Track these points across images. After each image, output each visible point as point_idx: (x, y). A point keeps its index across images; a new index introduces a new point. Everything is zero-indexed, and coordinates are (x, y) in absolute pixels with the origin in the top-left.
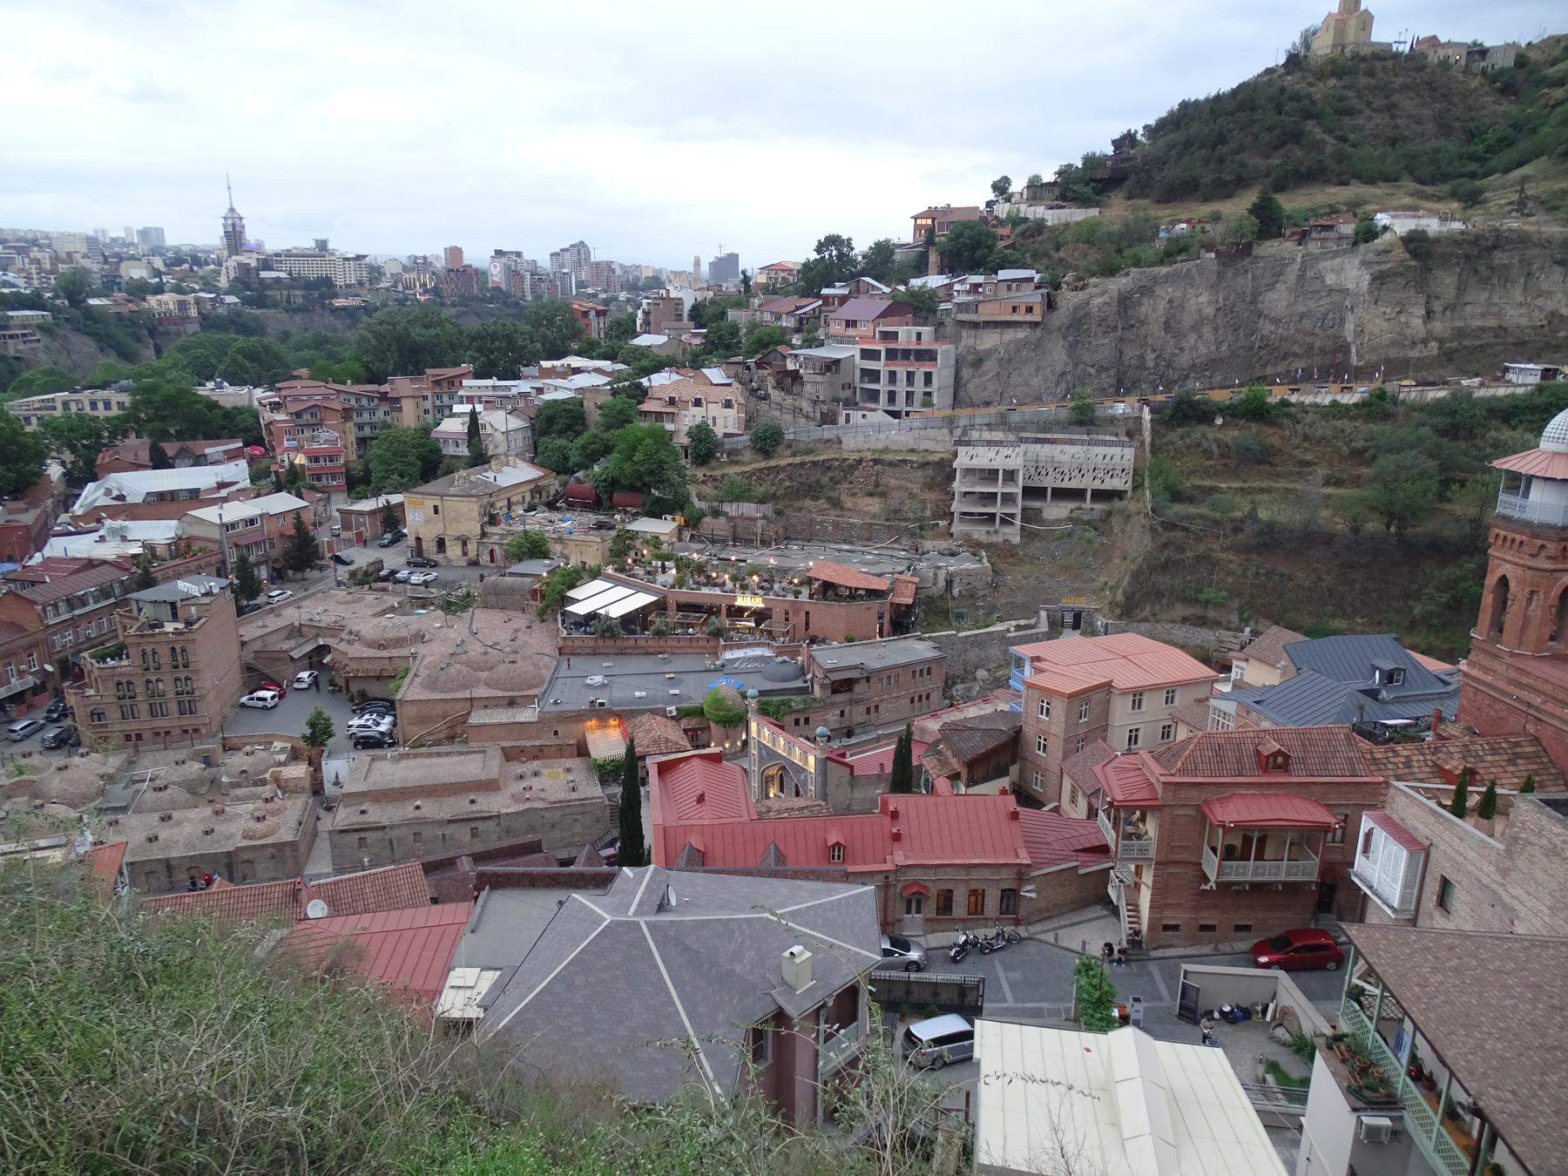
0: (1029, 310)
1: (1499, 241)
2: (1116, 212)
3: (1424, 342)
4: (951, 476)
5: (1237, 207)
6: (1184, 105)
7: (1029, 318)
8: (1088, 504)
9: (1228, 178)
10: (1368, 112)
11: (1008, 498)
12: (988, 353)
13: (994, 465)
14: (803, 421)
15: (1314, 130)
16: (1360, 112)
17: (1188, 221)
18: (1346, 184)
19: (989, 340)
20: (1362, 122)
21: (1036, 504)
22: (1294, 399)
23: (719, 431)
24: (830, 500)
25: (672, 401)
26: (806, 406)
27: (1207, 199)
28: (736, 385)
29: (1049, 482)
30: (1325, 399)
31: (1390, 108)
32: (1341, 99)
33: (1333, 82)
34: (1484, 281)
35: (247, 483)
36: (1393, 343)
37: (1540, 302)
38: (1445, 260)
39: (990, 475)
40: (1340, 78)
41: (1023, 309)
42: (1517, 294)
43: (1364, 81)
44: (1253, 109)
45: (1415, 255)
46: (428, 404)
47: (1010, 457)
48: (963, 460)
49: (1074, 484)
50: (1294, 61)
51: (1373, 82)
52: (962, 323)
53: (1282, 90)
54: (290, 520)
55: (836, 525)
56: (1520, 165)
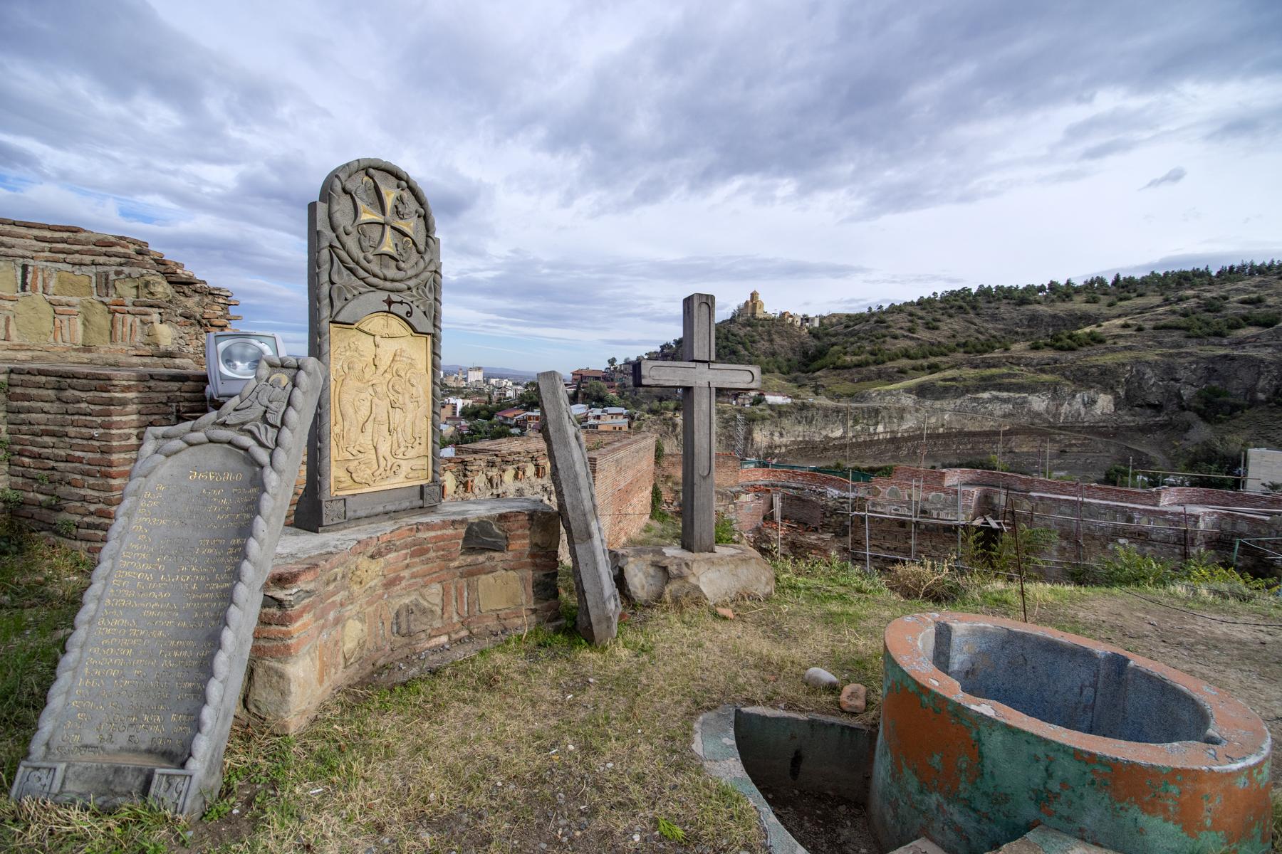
15: (740, 347)
31: (771, 341)
34: (799, 422)
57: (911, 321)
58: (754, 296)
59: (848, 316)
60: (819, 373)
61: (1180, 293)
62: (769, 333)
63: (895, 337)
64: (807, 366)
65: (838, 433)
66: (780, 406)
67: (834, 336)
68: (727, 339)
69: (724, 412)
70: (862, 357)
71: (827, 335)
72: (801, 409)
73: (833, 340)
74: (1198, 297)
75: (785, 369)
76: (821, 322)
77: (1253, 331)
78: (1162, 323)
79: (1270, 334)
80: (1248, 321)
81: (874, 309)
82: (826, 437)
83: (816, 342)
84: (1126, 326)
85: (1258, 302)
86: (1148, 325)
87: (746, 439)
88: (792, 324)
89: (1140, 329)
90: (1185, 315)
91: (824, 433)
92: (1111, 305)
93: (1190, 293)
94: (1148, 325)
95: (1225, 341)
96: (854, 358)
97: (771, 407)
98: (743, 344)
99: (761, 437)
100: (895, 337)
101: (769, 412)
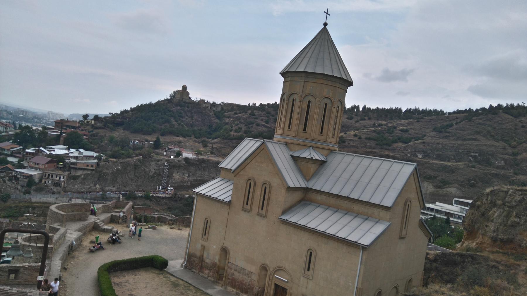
0: (92, 166)
1: (203, 161)
3: (188, 182)
5: (151, 139)
7: (91, 168)
9: (150, 130)
10: (186, 117)
12: (79, 176)
14: (18, 192)
15: (172, 119)
18: (178, 136)
19: (79, 173)
20: (184, 119)
26: (19, 187)
27: (144, 134)
31: (192, 117)
32: (181, 113)
33: (179, 107)
34: (200, 170)
36: (181, 181)
40: (181, 107)
41: (90, 166)
42: (207, 173)
43: (186, 109)
45: (186, 162)
53: (166, 108)
56: (216, 138)
57: (268, 117)
58: (184, 88)
59: (239, 106)
60: (216, 140)
61: (380, 122)
63: (258, 125)
64: (210, 134)
67: (229, 117)
70: (240, 134)
71: (224, 116)
73: (227, 120)
74: (386, 125)
76: (222, 109)
77: (400, 145)
78: (369, 136)
79: (404, 147)
80: (400, 140)
81: (251, 105)
83: (218, 121)
84: (355, 135)
85: (406, 131)
86: (363, 137)
88: (205, 108)
89: (360, 138)
90: (378, 133)
92: (357, 122)
93: (384, 122)
94: (363, 137)
95: (390, 148)
96: (235, 134)
97: (186, 159)
100: (258, 125)
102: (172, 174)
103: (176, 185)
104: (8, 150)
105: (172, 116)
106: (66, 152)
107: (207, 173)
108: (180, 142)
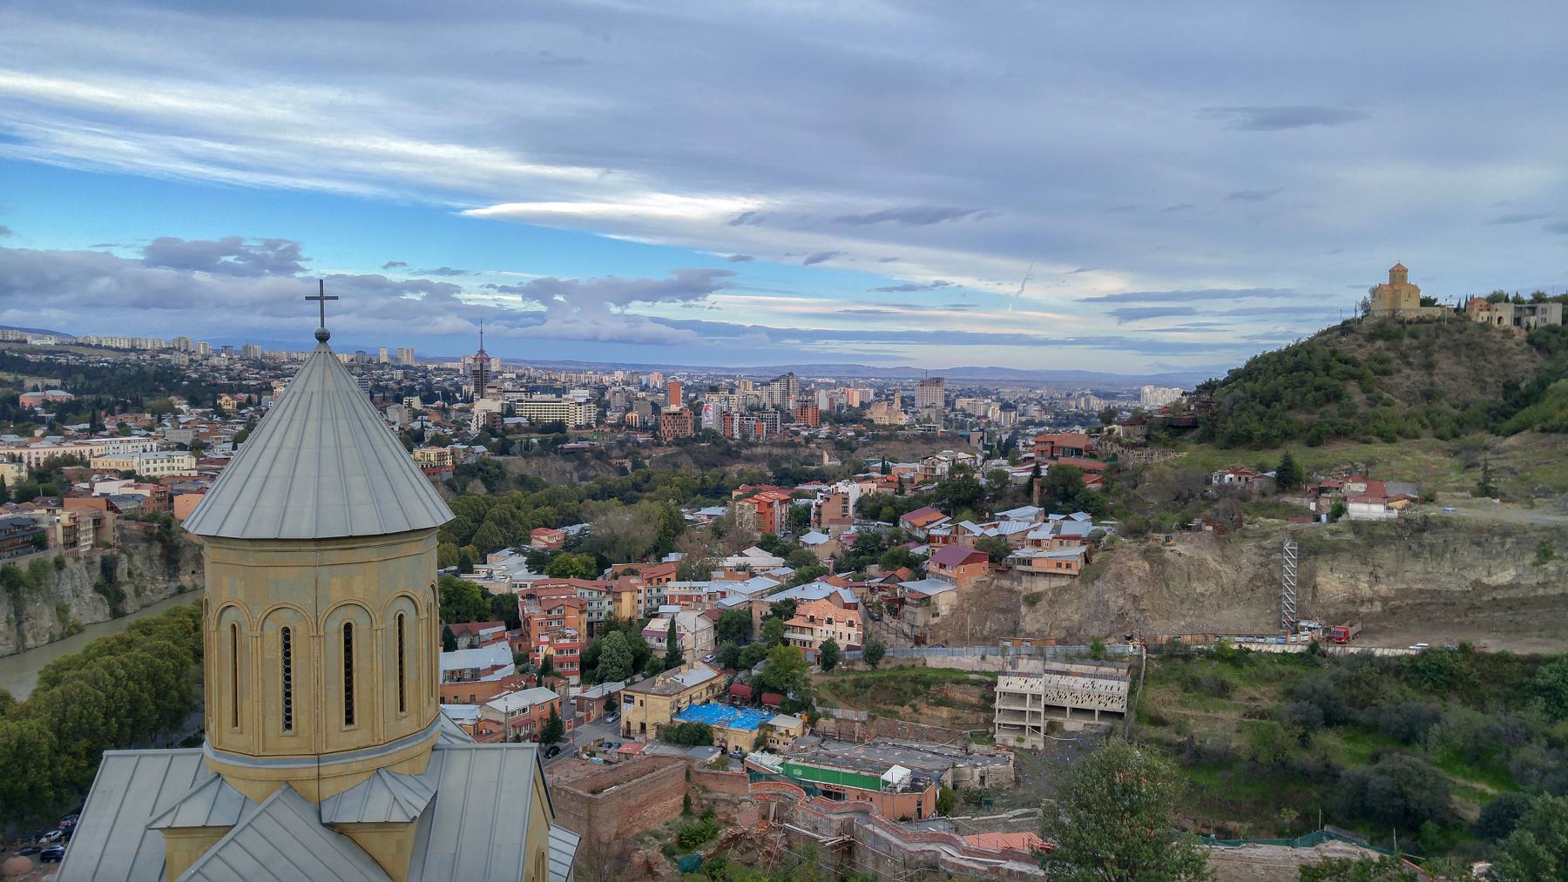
2: (1186, 456)
4: (993, 700)
5: (1274, 458)
6: (1255, 360)
7: (1068, 572)
8: (1096, 721)
10: (1408, 371)
11: (1035, 714)
13: (1024, 691)
15: (1352, 388)
16: (1399, 371)
17: (1235, 471)
19: (1041, 585)
21: (1059, 719)
22: (1253, 647)
23: (842, 644)
24: (913, 706)
25: (812, 619)
27: (1259, 448)
28: (861, 607)
29: (1068, 703)
30: (1278, 649)
33: (1380, 343)
34: (1416, 556)
35: (510, 669)
37: (1466, 573)
38: (1385, 540)
39: (1023, 696)
42: (1447, 568)
44: (1308, 369)
46: (641, 596)
47: (1037, 686)
48: (1003, 684)
49: (1085, 706)
50: (1346, 328)
51: (1415, 342)
52: (1023, 572)
53: (1334, 353)
54: (548, 708)
55: (911, 728)
56: (1515, 432)
62: (1427, 350)
65: (1505, 576)
66: (1373, 524)
68: (1327, 369)
69: (1266, 536)
72: (1421, 530)
75: (1445, 430)
82: (1477, 583)
87: (1301, 583)
91: (1472, 576)
97: (1357, 526)
98: (1359, 378)
99: (1333, 582)
101: (1350, 536)
102: (1312, 575)
103: (1332, 612)
104: (922, 528)
105: (1353, 377)
106: (1025, 526)
107: (1447, 568)
108: (1370, 464)
